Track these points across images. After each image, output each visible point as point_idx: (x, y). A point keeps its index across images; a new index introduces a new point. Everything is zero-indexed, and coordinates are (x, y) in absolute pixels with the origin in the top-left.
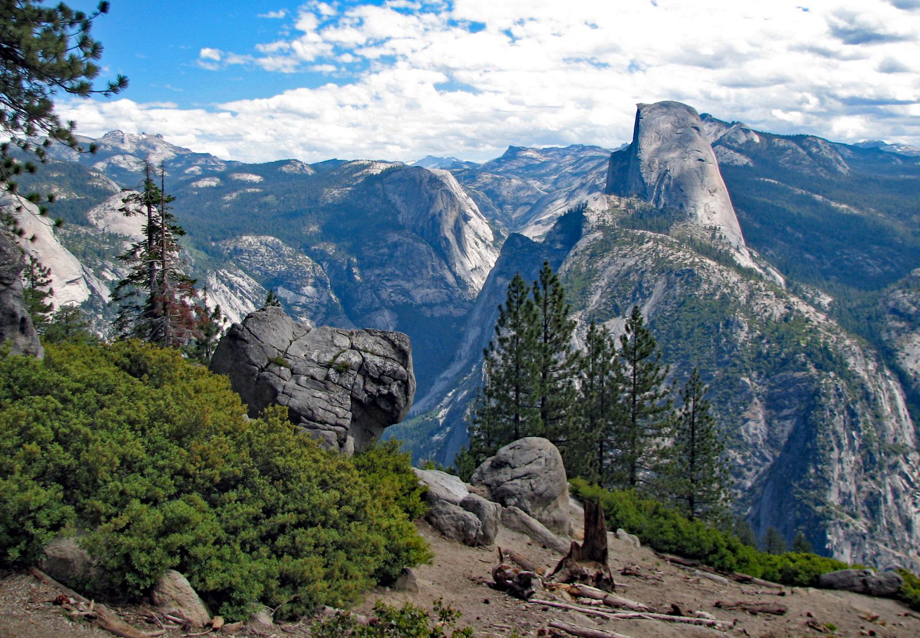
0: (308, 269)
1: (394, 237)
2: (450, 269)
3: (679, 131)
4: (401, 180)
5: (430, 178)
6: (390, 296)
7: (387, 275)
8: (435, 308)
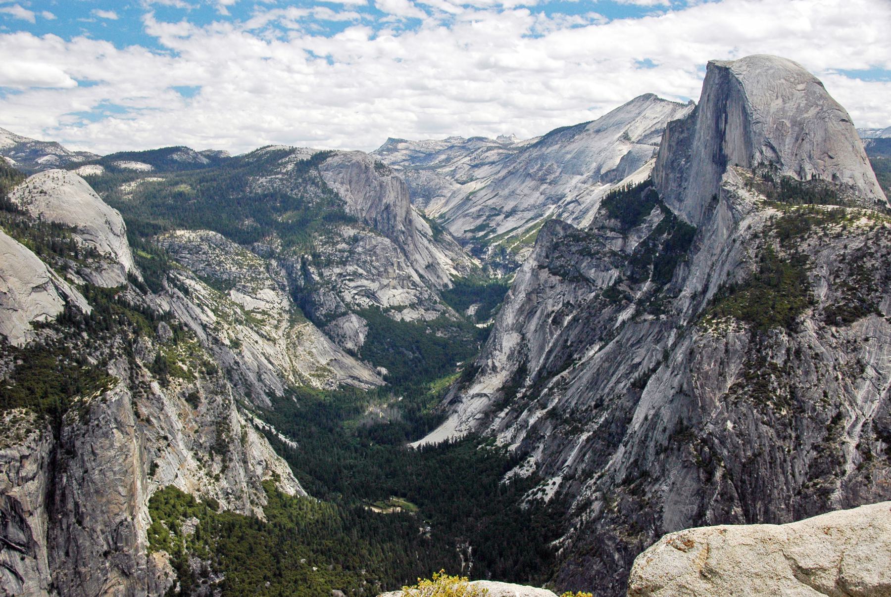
0: (262, 269)
1: (349, 232)
2: (411, 264)
4: (341, 166)
5: (376, 164)
6: (353, 297)
7: (350, 275)
8: (405, 311)
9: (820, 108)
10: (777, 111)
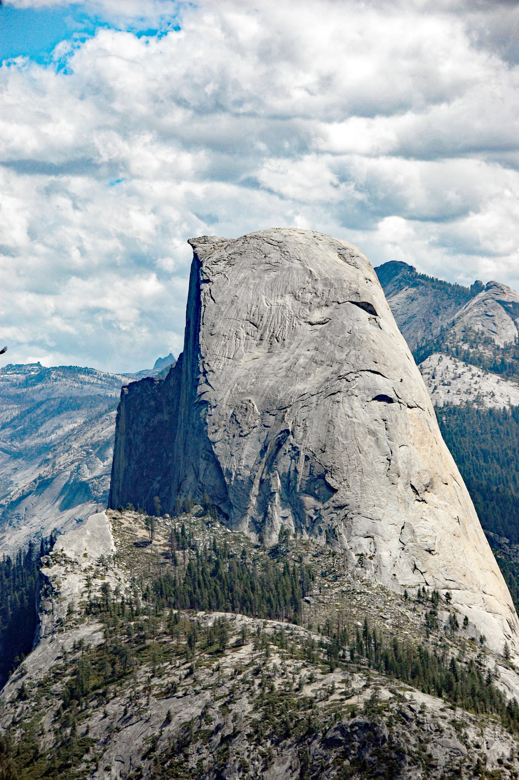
3: (317, 316)
9: (336, 367)
10: (246, 376)
